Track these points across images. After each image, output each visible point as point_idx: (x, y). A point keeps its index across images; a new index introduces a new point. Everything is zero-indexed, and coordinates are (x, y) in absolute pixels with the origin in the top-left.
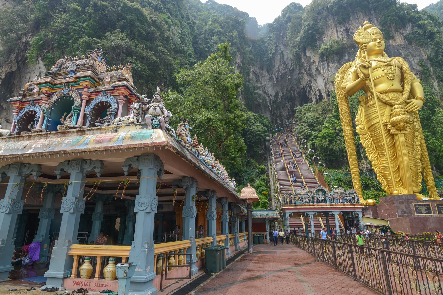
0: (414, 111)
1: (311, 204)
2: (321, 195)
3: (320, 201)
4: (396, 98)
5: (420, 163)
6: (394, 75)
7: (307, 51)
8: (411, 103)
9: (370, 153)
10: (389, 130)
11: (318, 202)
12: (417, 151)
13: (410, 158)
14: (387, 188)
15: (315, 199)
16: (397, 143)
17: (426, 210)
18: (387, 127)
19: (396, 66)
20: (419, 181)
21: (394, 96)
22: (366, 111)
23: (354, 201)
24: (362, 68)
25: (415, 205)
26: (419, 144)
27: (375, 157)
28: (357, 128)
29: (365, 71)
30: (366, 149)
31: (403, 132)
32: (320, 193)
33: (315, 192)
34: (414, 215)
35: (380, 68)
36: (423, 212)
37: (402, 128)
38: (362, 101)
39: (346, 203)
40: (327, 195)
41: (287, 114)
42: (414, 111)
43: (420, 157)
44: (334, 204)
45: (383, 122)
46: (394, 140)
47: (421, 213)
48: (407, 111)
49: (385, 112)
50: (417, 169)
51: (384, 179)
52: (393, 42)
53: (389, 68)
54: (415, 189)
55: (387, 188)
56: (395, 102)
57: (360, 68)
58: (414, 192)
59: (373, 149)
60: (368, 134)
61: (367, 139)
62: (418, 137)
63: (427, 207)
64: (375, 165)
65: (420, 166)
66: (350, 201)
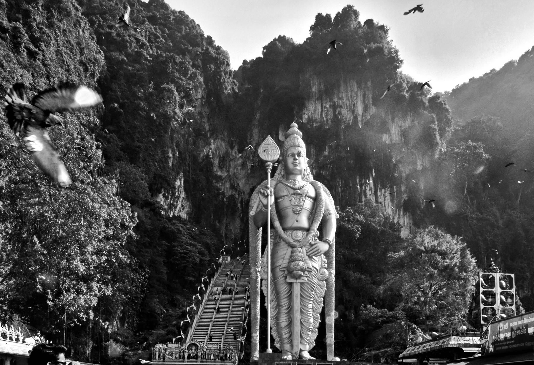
4: (298, 239)
7: (280, 132)
8: (314, 247)
10: (286, 277)
16: (293, 293)
18: (284, 273)
30: (266, 298)
37: (297, 277)
45: (281, 267)
46: (291, 290)
48: (309, 256)
49: (286, 254)
52: (388, 138)
56: (295, 243)
58: (301, 351)
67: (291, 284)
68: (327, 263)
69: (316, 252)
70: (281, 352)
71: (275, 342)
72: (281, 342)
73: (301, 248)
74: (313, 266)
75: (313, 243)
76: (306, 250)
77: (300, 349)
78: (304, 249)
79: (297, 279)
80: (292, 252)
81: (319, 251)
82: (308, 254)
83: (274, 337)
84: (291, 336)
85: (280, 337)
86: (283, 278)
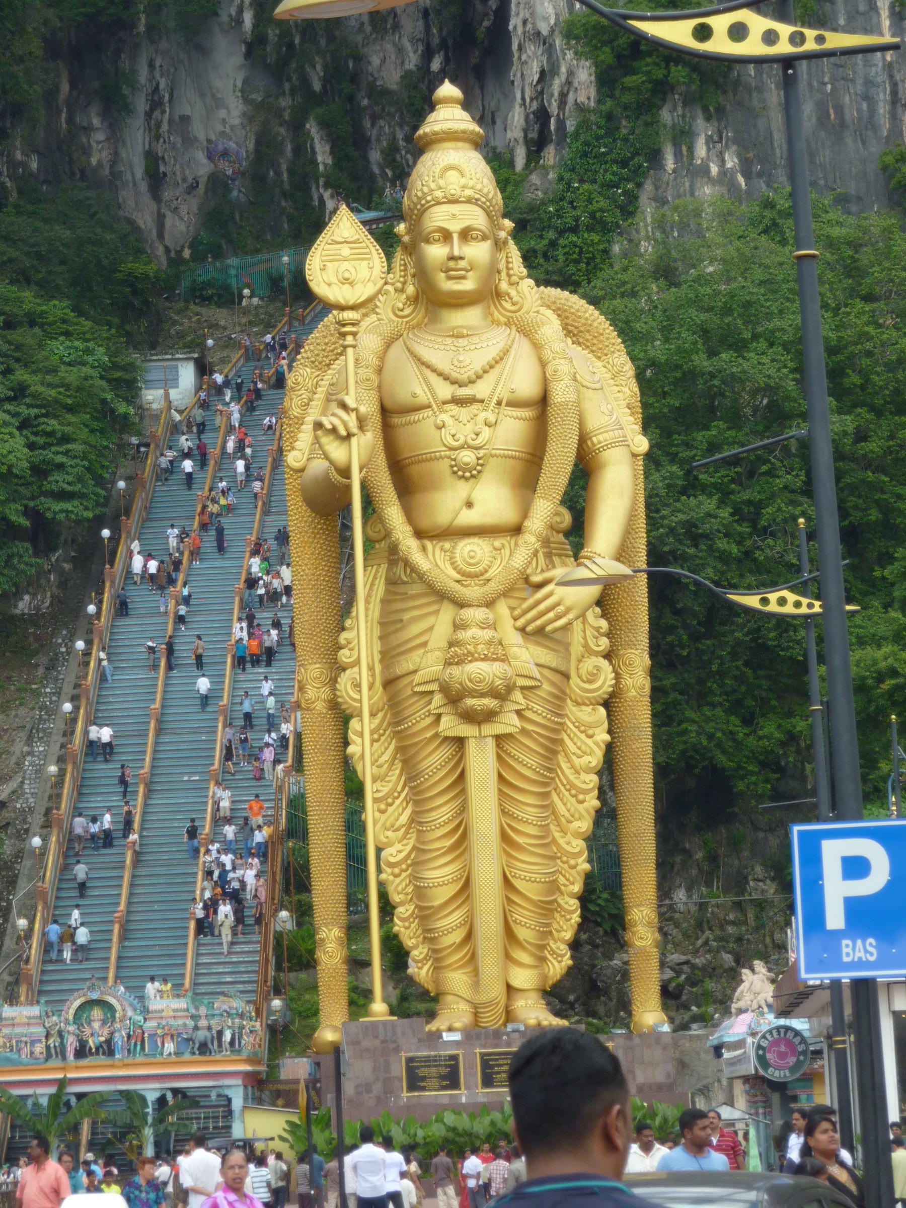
0: (548, 628)
1: (55, 1062)
2: (96, 1025)
3: (90, 1049)
4: (478, 569)
5: (578, 855)
6: (482, 453)
9: (383, 807)
11: (82, 1052)
12: (581, 797)
13: (520, 840)
14: (426, 968)
15: (71, 1043)
17: (442, 1077)
19: (499, 403)
20: (563, 934)
21: (472, 558)
22: (384, 602)
23: (220, 1045)
24: (324, 435)
25: (410, 1060)
26: (594, 764)
27: (398, 830)
28: (344, 681)
29: (338, 452)
31: (490, 729)
32: (97, 1013)
33: (72, 1011)
34: (398, 1097)
35: (428, 412)
36: (435, 1083)
38: (379, 541)
39: (187, 1056)
40: (117, 1025)
41: (412, 60)
42: (548, 628)
43: (585, 825)
44: (139, 1059)
47: (423, 1089)
48: (522, 630)
49: (431, 629)
50: (553, 887)
51: (419, 932)
53: (464, 413)
54: (523, 978)
55: (426, 968)
57: (319, 433)
59: (394, 790)
60: (380, 715)
61: (377, 741)
62: (597, 731)
63: (446, 1066)
64: (392, 865)
65: (579, 868)
66: (204, 1048)
67: (460, 742)
68: (609, 635)
69: (551, 615)
70: (436, 999)
71: (410, 961)
72: (437, 958)
73: (489, 604)
74: (537, 665)
75: (537, 579)
76: (512, 609)
77: (509, 988)
78: (502, 608)
79: (479, 724)
80: (458, 626)
81: (560, 609)
82: (520, 623)
83: (409, 942)
84: (469, 936)
85: (429, 937)
86: (428, 721)
